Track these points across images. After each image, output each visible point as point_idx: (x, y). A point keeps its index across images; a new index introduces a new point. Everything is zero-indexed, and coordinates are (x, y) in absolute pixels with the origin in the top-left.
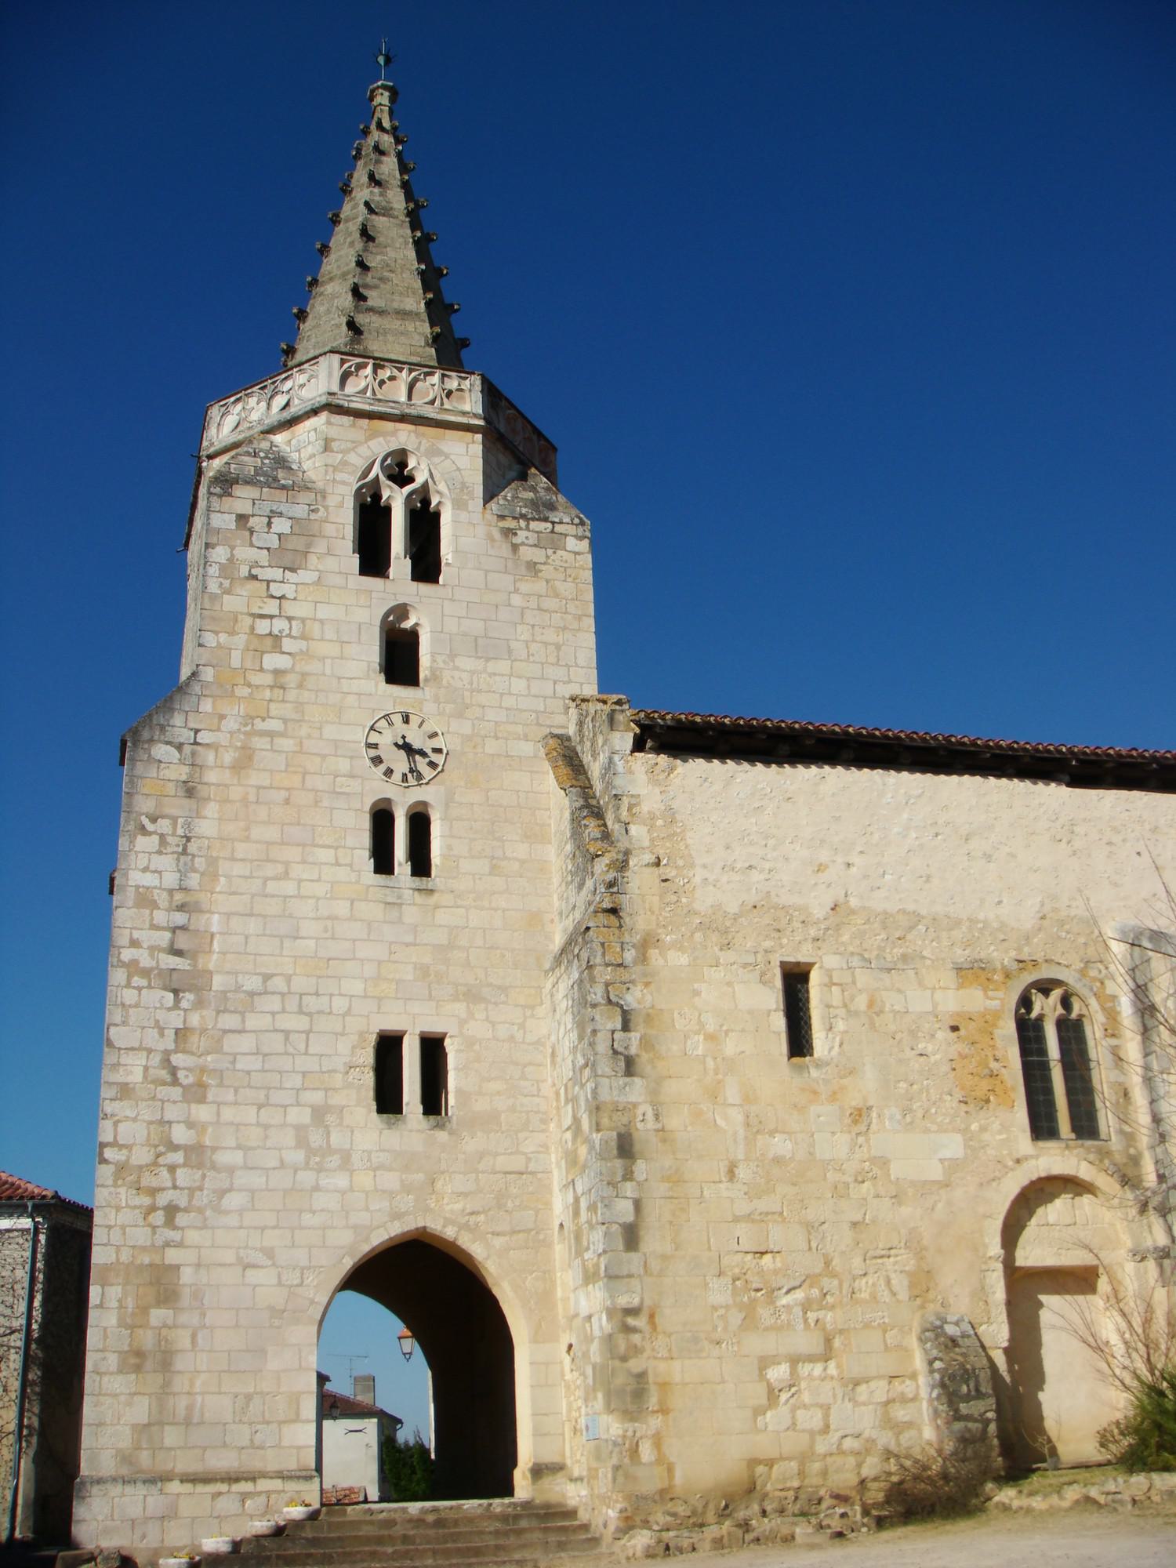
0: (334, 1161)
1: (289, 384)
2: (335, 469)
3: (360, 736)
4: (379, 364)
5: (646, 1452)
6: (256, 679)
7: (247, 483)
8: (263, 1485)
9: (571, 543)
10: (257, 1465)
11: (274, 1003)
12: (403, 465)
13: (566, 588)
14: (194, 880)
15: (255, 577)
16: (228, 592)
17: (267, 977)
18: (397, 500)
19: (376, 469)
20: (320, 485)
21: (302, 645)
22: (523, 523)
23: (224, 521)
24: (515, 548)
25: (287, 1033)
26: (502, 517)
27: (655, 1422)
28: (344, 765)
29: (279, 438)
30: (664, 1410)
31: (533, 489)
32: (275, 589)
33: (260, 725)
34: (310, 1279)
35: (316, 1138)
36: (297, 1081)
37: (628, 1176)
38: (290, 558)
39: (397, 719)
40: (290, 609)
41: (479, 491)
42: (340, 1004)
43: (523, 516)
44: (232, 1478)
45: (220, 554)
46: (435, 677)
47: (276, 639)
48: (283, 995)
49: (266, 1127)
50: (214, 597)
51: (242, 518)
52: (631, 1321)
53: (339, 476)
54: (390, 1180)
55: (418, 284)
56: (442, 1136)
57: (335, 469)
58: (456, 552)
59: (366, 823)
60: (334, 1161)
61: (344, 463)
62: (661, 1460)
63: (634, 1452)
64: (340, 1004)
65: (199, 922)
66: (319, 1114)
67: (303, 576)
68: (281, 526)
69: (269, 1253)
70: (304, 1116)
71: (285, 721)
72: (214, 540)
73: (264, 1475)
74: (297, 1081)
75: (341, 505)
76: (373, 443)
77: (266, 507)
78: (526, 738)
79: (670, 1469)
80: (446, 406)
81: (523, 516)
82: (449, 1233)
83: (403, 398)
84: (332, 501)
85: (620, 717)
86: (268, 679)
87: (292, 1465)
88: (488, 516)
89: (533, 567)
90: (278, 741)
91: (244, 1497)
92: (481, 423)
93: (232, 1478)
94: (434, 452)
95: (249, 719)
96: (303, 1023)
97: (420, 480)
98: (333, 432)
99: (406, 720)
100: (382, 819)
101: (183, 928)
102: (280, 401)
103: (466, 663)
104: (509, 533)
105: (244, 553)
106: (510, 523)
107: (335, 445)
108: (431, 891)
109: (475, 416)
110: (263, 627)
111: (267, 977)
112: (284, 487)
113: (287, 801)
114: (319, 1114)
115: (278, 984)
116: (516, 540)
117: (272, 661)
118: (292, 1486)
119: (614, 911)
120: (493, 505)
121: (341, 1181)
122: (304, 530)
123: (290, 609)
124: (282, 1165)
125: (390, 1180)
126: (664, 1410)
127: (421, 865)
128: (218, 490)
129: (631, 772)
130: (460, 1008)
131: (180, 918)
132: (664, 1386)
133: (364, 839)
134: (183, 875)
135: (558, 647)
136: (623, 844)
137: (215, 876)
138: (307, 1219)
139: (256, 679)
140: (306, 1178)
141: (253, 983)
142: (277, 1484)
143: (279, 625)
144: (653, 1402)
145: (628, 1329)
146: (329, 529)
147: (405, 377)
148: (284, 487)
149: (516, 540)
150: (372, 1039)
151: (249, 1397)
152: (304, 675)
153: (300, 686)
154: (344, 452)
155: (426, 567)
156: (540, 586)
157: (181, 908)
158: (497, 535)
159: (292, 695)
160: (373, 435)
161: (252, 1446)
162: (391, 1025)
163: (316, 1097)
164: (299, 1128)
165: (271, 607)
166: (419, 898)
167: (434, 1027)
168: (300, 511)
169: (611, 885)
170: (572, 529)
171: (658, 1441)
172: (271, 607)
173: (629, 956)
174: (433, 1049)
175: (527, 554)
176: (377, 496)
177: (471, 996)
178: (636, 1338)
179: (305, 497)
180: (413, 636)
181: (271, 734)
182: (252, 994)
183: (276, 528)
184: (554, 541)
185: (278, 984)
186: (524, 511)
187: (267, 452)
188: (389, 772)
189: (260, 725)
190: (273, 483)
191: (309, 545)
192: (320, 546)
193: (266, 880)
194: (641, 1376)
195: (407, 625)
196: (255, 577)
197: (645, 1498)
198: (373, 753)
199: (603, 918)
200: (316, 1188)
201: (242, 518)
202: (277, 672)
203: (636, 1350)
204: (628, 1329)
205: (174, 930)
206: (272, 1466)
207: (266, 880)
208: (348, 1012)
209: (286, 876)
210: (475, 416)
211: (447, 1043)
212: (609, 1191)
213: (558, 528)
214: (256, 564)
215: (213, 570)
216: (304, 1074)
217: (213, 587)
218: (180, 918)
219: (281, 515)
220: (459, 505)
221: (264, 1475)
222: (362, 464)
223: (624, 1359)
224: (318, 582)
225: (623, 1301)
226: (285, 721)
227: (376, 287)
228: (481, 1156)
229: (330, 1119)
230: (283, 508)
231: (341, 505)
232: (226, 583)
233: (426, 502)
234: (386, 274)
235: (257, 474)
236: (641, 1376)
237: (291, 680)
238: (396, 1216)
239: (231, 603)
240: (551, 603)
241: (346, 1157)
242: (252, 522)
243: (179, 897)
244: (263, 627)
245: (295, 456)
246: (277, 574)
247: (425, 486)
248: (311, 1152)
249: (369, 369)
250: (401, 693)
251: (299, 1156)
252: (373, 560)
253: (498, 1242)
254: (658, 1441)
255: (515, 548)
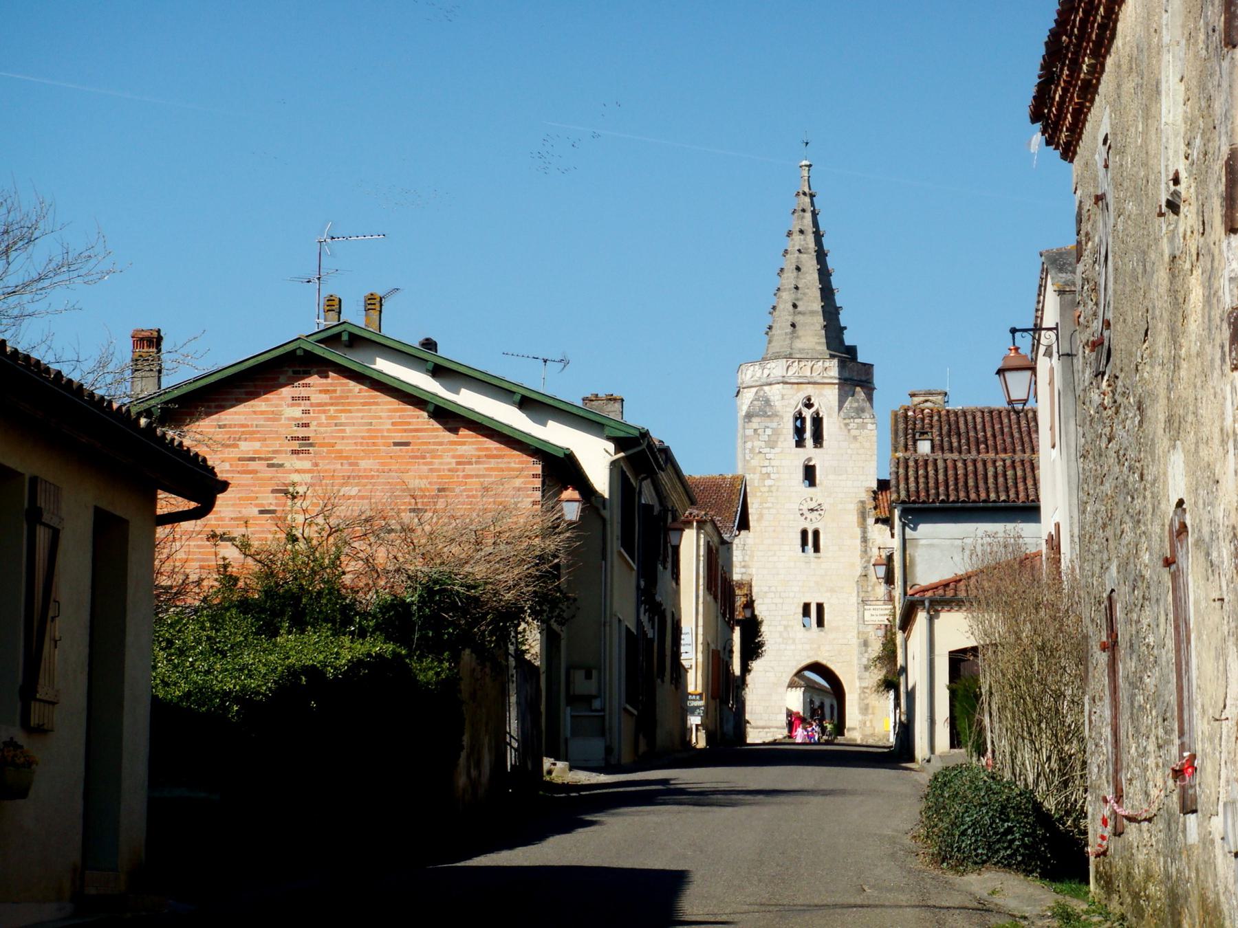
0: (791, 641)
1: (768, 366)
2: (786, 406)
3: (796, 507)
4: (800, 360)
5: (868, 724)
6: (763, 489)
7: (757, 416)
8: (772, 730)
9: (870, 426)
10: (771, 725)
11: (772, 595)
12: (809, 399)
13: (867, 445)
14: (747, 558)
15: (760, 452)
16: (752, 459)
17: (770, 587)
18: (808, 414)
19: (800, 405)
20: (780, 414)
21: (777, 476)
22: (852, 420)
23: (749, 432)
24: (849, 430)
25: (776, 604)
26: (844, 419)
27: (870, 716)
28: (792, 517)
29: (766, 388)
30: (873, 714)
31: (857, 401)
32: (768, 456)
33: (765, 505)
34: (784, 675)
35: (785, 635)
36: (779, 618)
37: (866, 652)
38: (771, 444)
39: (808, 500)
40: (773, 463)
41: (837, 408)
42: (792, 594)
43: (852, 417)
44: (763, 728)
45: (749, 445)
46: (821, 484)
47: (768, 474)
48: (774, 592)
49: (771, 632)
50: (748, 461)
51: (755, 430)
52: (865, 690)
53: (788, 409)
54: (807, 647)
55: (818, 294)
56: (822, 633)
57: (786, 406)
58: (828, 435)
59: (799, 536)
60: (791, 641)
61: (789, 404)
62: (872, 726)
63: (865, 723)
64: (792, 594)
65: (749, 571)
66: (786, 627)
67: (777, 450)
68: (769, 432)
69: (772, 668)
70: (781, 628)
71: (773, 503)
72: (747, 440)
73: (772, 727)
74: (779, 618)
75: (788, 421)
76: (799, 394)
77: (763, 425)
78: (851, 503)
79: (874, 729)
80: (825, 375)
81: (852, 417)
82: (824, 662)
83: (808, 374)
84: (785, 420)
85: (871, 513)
86: (766, 489)
87: (779, 725)
88: (840, 419)
89: (855, 438)
90: (771, 510)
91: (767, 733)
92: (837, 381)
93: (763, 728)
94: (821, 395)
95: (761, 503)
96: (781, 601)
97: (816, 406)
98: (784, 392)
99: (811, 499)
100: (804, 533)
101: (745, 573)
102: (766, 372)
103: (831, 477)
104: (847, 425)
105: (757, 444)
106: (847, 421)
107: (785, 397)
108: (819, 558)
109: (835, 378)
110: (764, 470)
111: (770, 587)
112: (769, 416)
113: (774, 531)
114: (786, 627)
115: (773, 589)
116: (850, 428)
117: (768, 482)
118: (780, 730)
119: (866, 576)
120: (842, 413)
121: (793, 647)
122: (776, 432)
123: (773, 463)
124: (776, 643)
125: (807, 647)
126: (873, 714)
127: (817, 548)
128: (746, 420)
129: (873, 531)
130: (828, 594)
131: (743, 570)
132: (874, 707)
133: (799, 541)
134: (744, 556)
135: (863, 467)
136: (869, 554)
137: (753, 557)
138: (783, 658)
139: (763, 489)
140: (783, 646)
141: (766, 589)
142: (776, 730)
143: (769, 469)
144: (870, 711)
145: (864, 693)
146: (784, 431)
147: (810, 364)
148: (769, 416)
149: (850, 428)
150: (802, 605)
151: (768, 707)
152: (778, 486)
153: (777, 490)
154: (789, 399)
155: (818, 439)
156: (858, 445)
157: (744, 567)
158: (843, 426)
159: (774, 494)
160: (798, 390)
161: (769, 719)
162: (807, 601)
163: (784, 623)
164: (780, 633)
165: (767, 463)
166: (816, 560)
167: (820, 601)
168: (774, 425)
169: (865, 567)
170: (870, 421)
171: (871, 721)
172: (767, 463)
173: (870, 589)
174: (820, 607)
175: (854, 432)
176: (800, 414)
177: (832, 590)
178: (867, 695)
179: (776, 419)
180: (813, 467)
181: (769, 508)
182: (766, 592)
183: (767, 433)
184: (863, 426)
185: (773, 589)
186: (853, 414)
187: (763, 397)
188: (806, 518)
189: (765, 505)
190: (765, 415)
191: (778, 438)
192: (781, 439)
193: (768, 556)
194: (868, 704)
195: (811, 463)
196: (760, 452)
197: (867, 735)
198: (801, 512)
199: (862, 578)
200: (785, 649)
201: (755, 430)
202: (770, 486)
203: (866, 698)
204: (864, 693)
205: (742, 574)
206: (775, 725)
207: (768, 556)
208: (795, 597)
209: (775, 555)
210: (835, 378)
211: (825, 605)
212: (861, 656)
213: (865, 421)
214: (761, 448)
215: (747, 451)
216: (782, 616)
217: (748, 458)
218: (743, 570)
219: (768, 427)
220: (829, 416)
221: (772, 727)
222: (795, 403)
223: (863, 700)
224: (781, 452)
225: (863, 685)
226: (773, 503)
227: (801, 299)
228: (834, 639)
229: (789, 629)
230: (769, 424)
231: (788, 421)
232: (752, 456)
233: (818, 414)
234: (806, 290)
235: (760, 411)
236: (868, 704)
237: (774, 489)
238: (809, 657)
239: (754, 463)
240: (861, 451)
241: (794, 640)
242: (759, 431)
243: (743, 564)
244: (764, 470)
245: (772, 397)
246: (768, 450)
247: (817, 410)
248: (783, 638)
249: (797, 363)
250: (812, 490)
251: (781, 640)
252: (800, 443)
253: (839, 664)
254: (871, 721)
255: (849, 430)
